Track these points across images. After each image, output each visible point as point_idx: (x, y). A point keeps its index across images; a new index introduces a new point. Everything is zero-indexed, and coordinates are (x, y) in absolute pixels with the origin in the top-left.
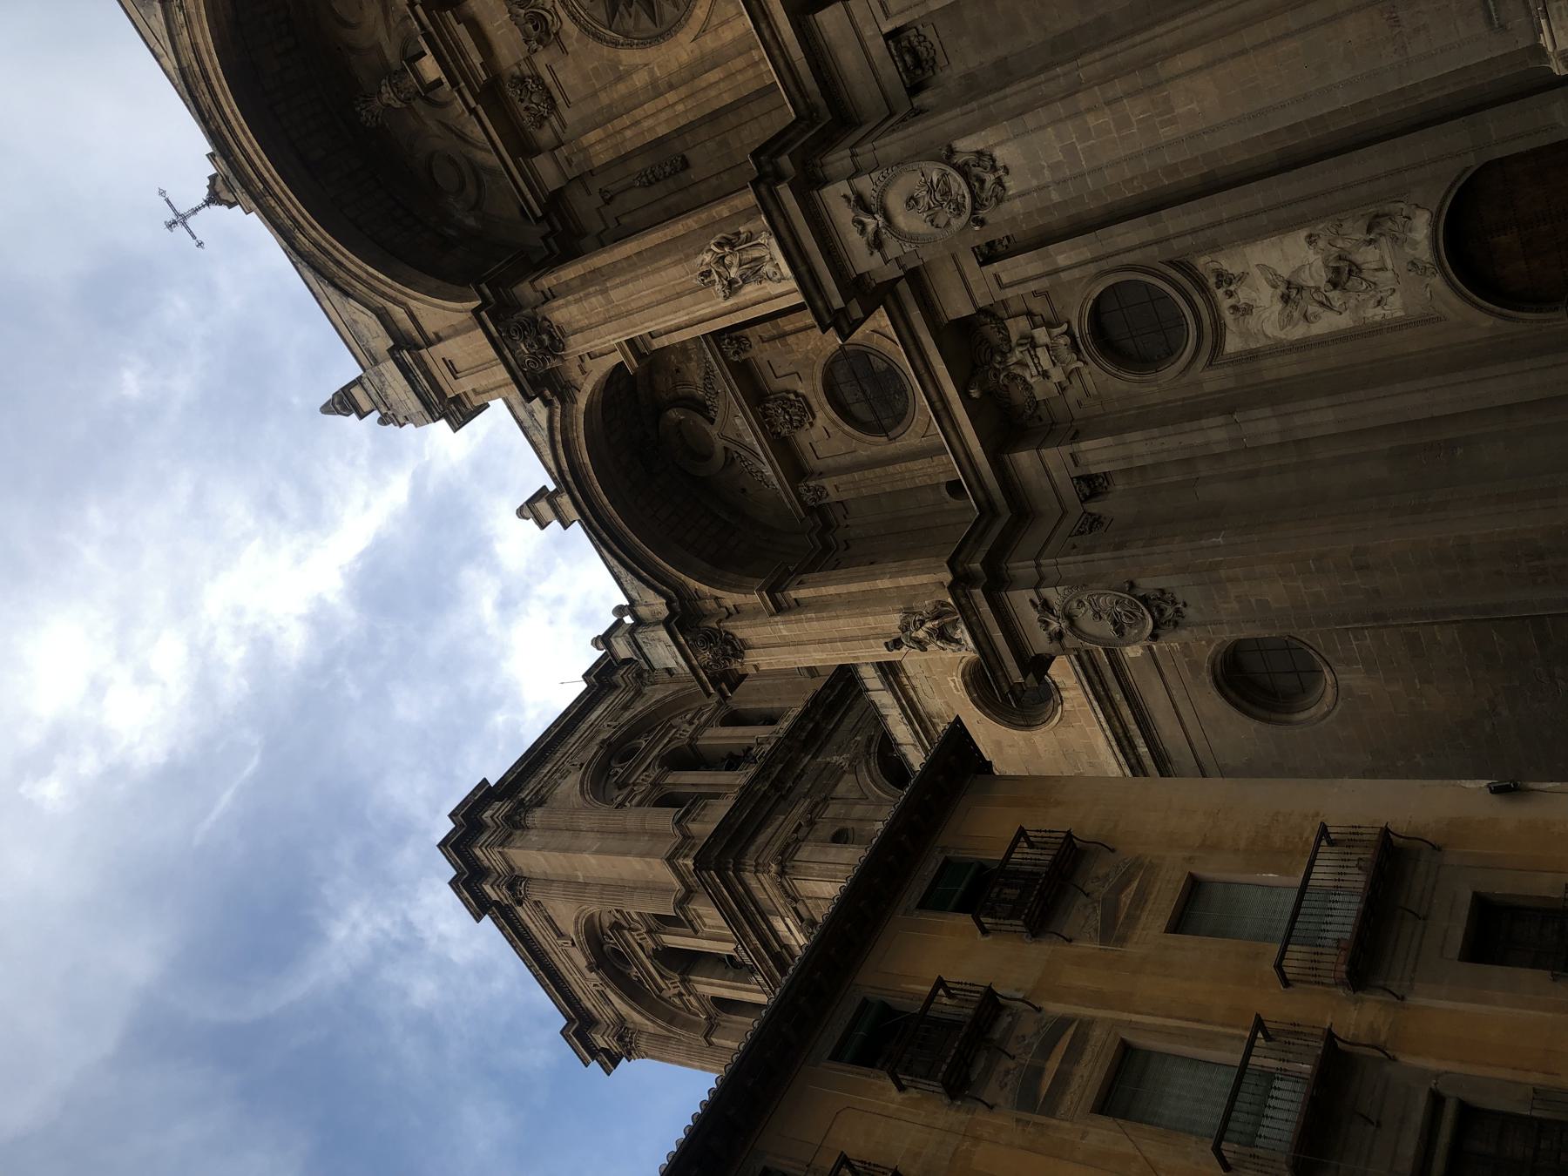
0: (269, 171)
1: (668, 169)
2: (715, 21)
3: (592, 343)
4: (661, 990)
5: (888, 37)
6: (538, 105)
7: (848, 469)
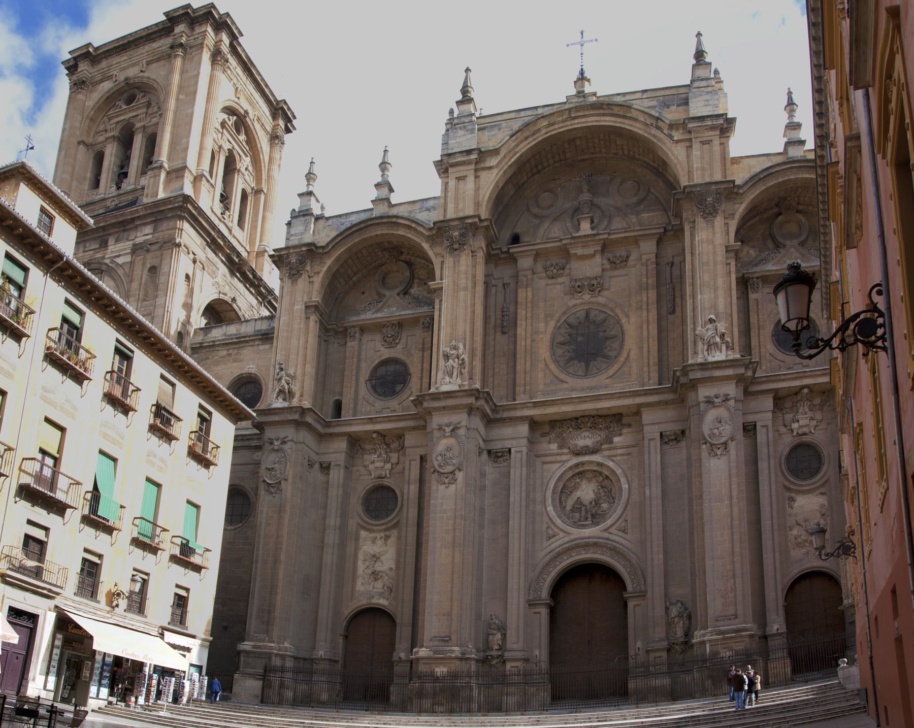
4: (110, 119)
7: (359, 355)
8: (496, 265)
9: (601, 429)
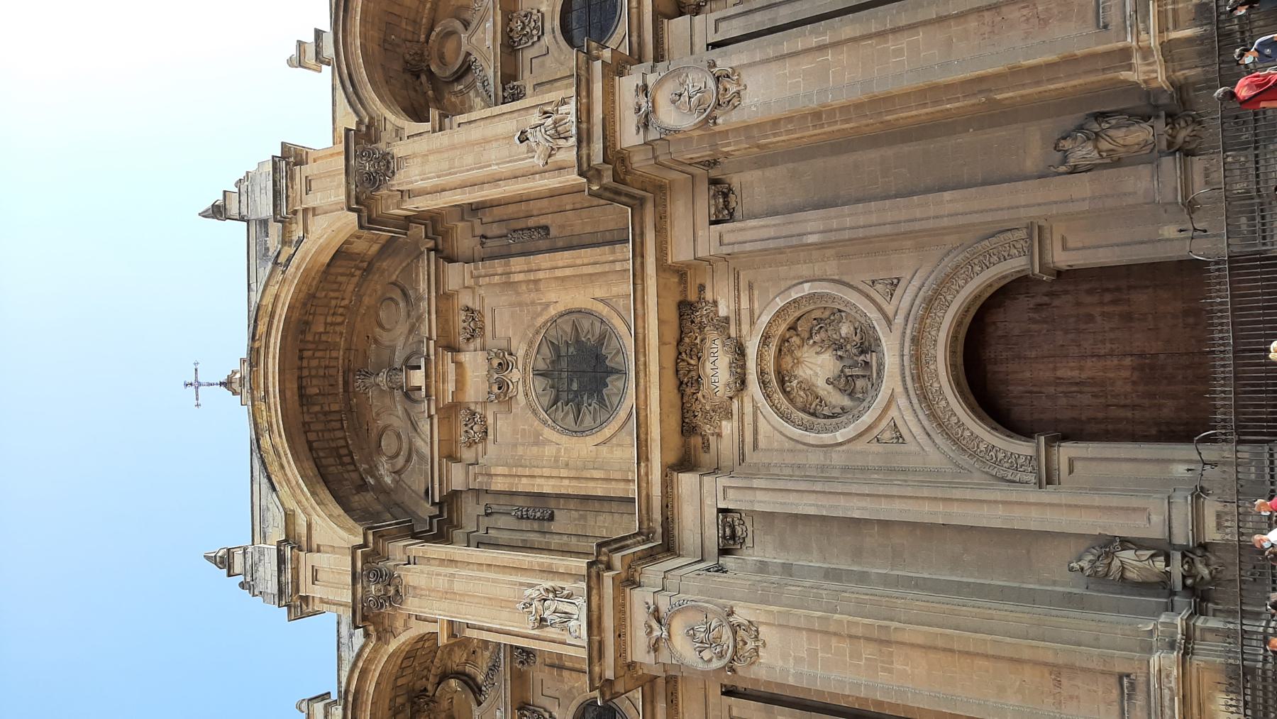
0: (274, 387)
1: (538, 514)
2: (614, 441)
3: (423, 610)
5: (720, 511)
6: (475, 433)
8: (459, 526)
9: (702, 341)
